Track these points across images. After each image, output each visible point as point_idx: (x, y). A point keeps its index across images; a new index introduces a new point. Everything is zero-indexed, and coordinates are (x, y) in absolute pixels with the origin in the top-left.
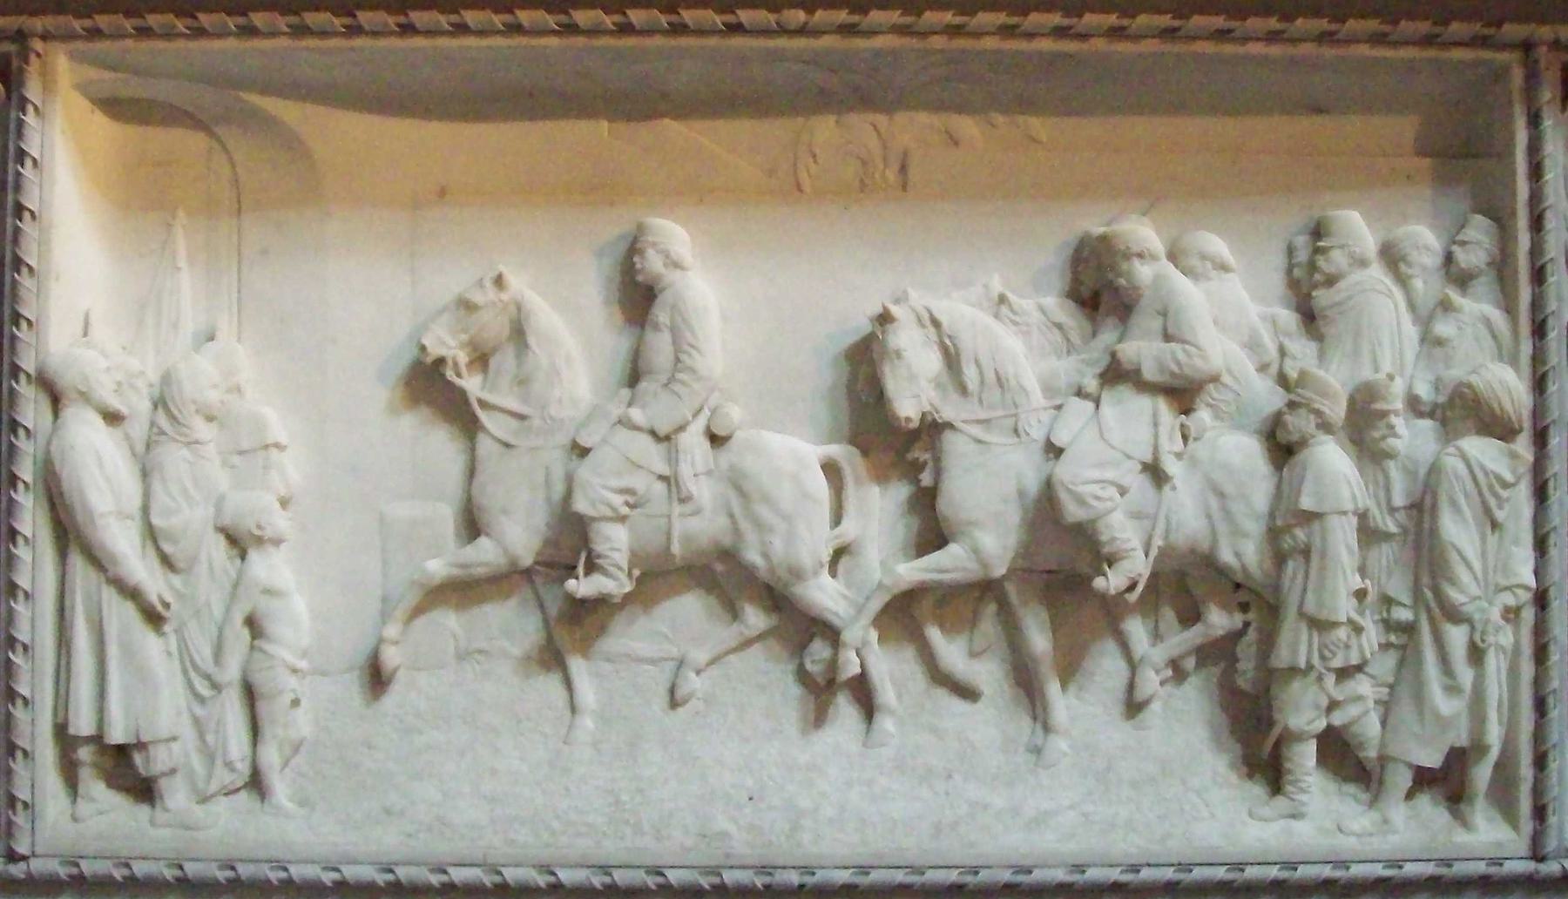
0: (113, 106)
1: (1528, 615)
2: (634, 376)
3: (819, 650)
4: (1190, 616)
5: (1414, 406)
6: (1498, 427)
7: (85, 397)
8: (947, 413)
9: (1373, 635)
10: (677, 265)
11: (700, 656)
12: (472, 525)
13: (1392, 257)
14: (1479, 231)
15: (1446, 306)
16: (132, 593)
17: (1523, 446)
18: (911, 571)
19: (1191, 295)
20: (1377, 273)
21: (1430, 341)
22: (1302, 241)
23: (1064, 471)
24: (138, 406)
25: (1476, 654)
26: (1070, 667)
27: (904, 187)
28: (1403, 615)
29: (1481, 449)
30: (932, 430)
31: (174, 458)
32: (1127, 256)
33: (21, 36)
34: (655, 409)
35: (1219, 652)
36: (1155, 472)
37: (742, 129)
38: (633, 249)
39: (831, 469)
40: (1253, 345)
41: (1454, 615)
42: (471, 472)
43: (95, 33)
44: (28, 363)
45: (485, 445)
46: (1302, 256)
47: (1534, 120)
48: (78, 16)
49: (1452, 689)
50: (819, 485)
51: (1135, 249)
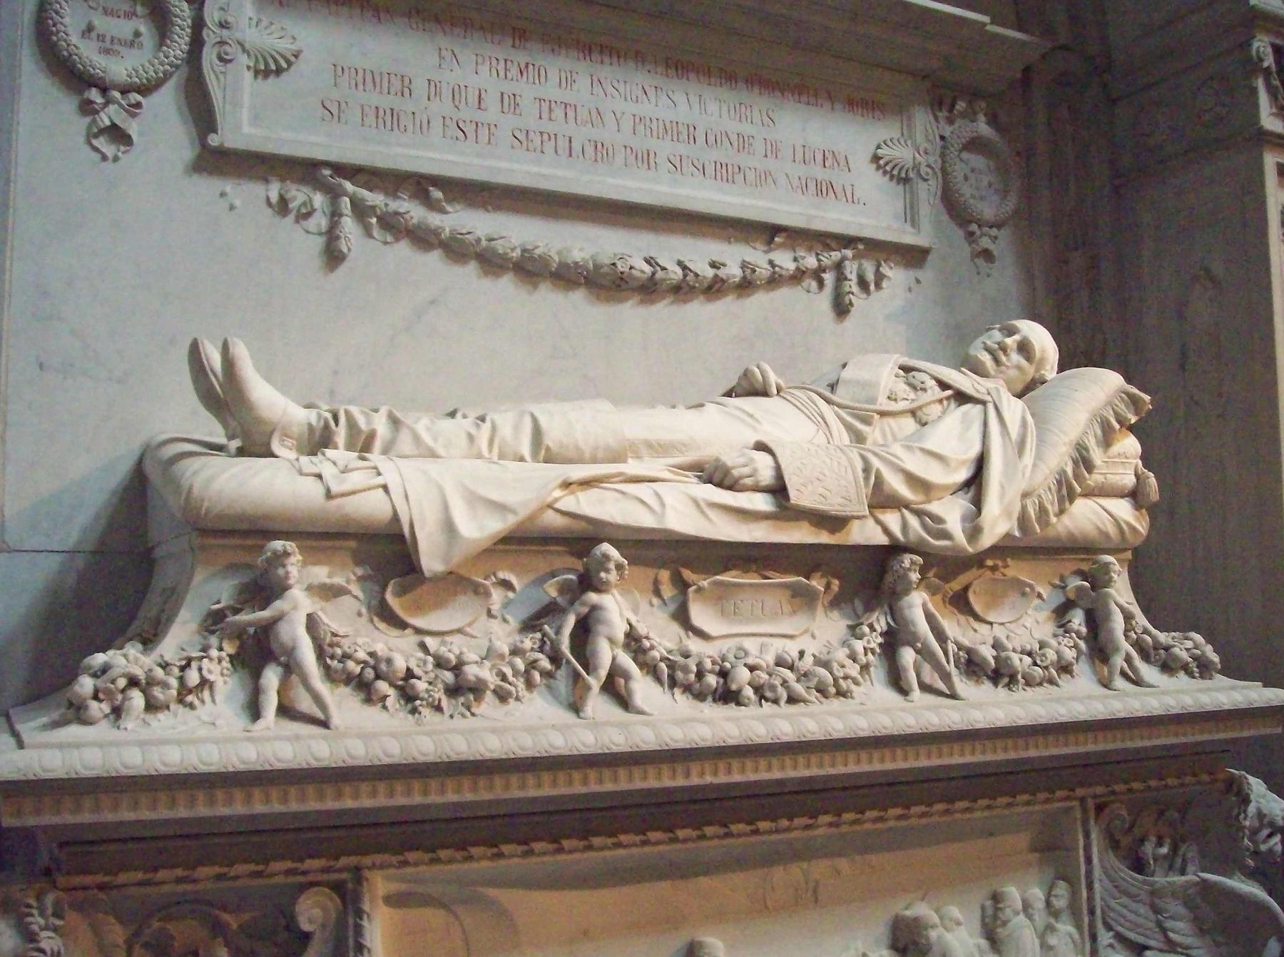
14: (1062, 889)
22: (989, 903)
27: (816, 901)
32: (926, 929)
33: (358, 869)
37: (738, 879)
43: (405, 863)
46: (990, 912)
48: (395, 854)
51: (931, 923)
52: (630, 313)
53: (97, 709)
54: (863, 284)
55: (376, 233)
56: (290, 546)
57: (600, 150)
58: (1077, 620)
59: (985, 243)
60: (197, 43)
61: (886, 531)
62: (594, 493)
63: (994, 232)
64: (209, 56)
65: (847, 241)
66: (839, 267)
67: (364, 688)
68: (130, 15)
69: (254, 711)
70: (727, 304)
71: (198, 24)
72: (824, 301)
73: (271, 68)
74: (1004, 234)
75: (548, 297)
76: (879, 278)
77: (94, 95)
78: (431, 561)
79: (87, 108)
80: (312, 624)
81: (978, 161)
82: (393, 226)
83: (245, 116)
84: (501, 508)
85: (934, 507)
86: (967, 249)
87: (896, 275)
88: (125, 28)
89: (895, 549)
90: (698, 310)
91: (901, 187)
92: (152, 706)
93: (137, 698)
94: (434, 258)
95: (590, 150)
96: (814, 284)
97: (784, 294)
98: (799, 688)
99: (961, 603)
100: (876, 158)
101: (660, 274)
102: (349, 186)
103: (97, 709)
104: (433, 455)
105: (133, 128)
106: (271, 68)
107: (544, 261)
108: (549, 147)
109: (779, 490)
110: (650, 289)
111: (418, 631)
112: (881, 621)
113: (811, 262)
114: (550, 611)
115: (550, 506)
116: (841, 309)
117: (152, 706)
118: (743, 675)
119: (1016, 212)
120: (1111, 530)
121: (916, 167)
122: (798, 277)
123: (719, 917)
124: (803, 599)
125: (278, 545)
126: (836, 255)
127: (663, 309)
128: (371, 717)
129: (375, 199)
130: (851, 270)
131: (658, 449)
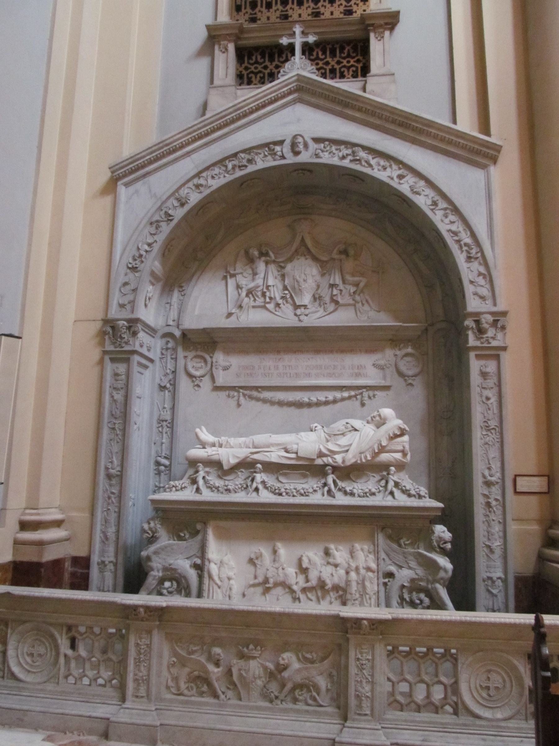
1: (377, 594)
2: (274, 561)
3: (294, 594)
4: (337, 592)
6: (373, 572)
7: (213, 562)
8: (309, 567)
9: (358, 596)
10: (279, 548)
11: (280, 594)
12: (255, 577)
13: (362, 550)
14: (372, 546)
15: (368, 556)
16: (217, 584)
17: (376, 574)
19: (337, 554)
21: (366, 560)
23: (322, 574)
24: (219, 562)
25: (370, 599)
26: (323, 598)
28: (361, 593)
29: (370, 574)
30: (307, 569)
31: (222, 569)
34: (277, 565)
35: (341, 597)
36: (332, 575)
39: (296, 573)
40: (345, 560)
41: (367, 594)
42: (256, 571)
44: (207, 558)
45: (258, 570)
47: (378, 534)
49: (367, 603)
50: (294, 574)
52: (305, 411)
53: (168, 490)
54: (369, 398)
55: (248, 399)
56: (201, 464)
57: (297, 375)
58: (383, 483)
59: (410, 381)
60: (212, 365)
61: (323, 461)
63: (414, 378)
64: (214, 369)
66: (362, 393)
68: (200, 362)
69: (192, 491)
71: (212, 363)
72: (358, 403)
73: (226, 369)
75: (285, 409)
76: (374, 396)
78: (226, 467)
79: (193, 381)
80: (204, 478)
82: (251, 397)
84: (238, 457)
86: (404, 384)
88: (199, 365)
89: (326, 465)
90: (323, 409)
91: (382, 371)
92: (177, 490)
93: (174, 489)
94: (259, 403)
95: (295, 376)
97: (346, 402)
98: (295, 494)
100: (374, 365)
101: (311, 402)
102: (241, 391)
103: (168, 490)
105: (201, 384)
106: (226, 369)
107: (283, 401)
108: (285, 376)
109: (297, 453)
110: (309, 405)
111: (225, 480)
113: (353, 393)
114: (250, 476)
115: (248, 457)
116: (363, 405)
118: (283, 490)
120: (393, 460)
121: (385, 365)
122: (350, 398)
123: (282, 539)
125: (199, 464)
126: (360, 391)
127: (313, 410)
128: (212, 494)
130: (366, 394)
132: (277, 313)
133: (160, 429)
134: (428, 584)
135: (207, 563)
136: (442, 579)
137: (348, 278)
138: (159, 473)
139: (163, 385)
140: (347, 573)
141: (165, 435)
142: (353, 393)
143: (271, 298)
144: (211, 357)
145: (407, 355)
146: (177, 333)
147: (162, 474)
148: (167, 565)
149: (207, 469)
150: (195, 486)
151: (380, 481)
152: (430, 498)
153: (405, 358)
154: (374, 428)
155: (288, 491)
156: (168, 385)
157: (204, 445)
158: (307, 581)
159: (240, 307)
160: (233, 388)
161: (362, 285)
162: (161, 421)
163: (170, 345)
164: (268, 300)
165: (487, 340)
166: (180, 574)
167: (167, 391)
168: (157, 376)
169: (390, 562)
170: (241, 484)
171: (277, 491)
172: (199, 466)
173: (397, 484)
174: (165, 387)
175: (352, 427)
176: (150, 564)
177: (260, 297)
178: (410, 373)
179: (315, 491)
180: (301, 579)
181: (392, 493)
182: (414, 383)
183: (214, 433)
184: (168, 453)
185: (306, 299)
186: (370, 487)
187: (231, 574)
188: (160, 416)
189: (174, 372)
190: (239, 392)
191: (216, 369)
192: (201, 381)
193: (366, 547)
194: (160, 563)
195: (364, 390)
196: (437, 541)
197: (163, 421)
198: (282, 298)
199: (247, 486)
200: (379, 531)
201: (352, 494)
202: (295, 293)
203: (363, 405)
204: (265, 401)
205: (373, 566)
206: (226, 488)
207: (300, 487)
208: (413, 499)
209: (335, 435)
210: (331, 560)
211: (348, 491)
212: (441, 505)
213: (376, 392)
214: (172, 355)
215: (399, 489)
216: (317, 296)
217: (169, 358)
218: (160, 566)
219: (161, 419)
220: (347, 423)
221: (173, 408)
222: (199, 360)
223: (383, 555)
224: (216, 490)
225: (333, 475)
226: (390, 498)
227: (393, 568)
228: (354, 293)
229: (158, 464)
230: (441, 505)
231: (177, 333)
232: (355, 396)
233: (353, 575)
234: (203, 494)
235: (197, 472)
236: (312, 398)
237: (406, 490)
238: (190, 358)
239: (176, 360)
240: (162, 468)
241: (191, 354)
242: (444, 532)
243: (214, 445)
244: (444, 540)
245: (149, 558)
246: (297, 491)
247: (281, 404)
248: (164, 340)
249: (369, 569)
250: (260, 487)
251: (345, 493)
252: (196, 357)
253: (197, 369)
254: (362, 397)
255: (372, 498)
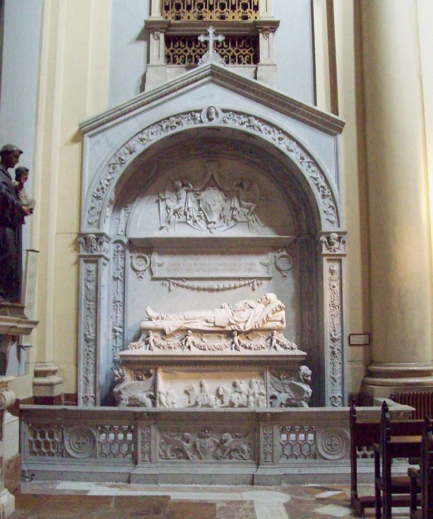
0: (163, 372)
2: (201, 391)
5: (258, 393)
6: (263, 395)
8: (224, 394)
12: (189, 402)
13: (257, 383)
14: (263, 381)
18: (221, 405)
19: (241, 386)
20: (256, 384)
21: (259, 389)
24: (165, 394)
30: (223, 395)
31: (168, 398)
34: (202, 394)
36: (238, 398)
38: (201, 382)
42: (189, 398)
45: (190, 397)
50: (215, 399)
52: (215, 294)
54: (258, 285)
57: (210, 270)
58: (269, 341)
59: (285, 274)
62: (189, 324)
65: (254, 278)
66: (253, 282)
67: (159, 347)
69: (146, 349)
70: (232, 290)
71: (150, 261)
72: (250, 288)
73: (160, 265)
74: (289, 272)
75: (202, 293)
76: (261, 284)
77: (138, 273)
78: (167, 333)
79: (137, 274)
80: (153, 340)
81: (284, 259)
82: (178, 285)
83: (157, 272)
84: (176, 326)
85: (239, 325)
86: (281, 276)
87: (264, 282)
88: (141, 263)
89: (233, 331)
90: (227, 293)
91: (266, 267)
93: (134, 348)
94: (184, 289)
96: (248, 286)
97: (243, 288)
98: (214, 349)
99: (248, 338)
102: (171, 280)
103: (130, 348)
104: (171, 320)
106: (160, 265)
109: (214, 323)
110: (218, 290)
112: (231, 340)
114: (183, 339)
116: (253, 290)
117: (136, 348)
118: (206, 347)
119: (292, 268)
120: (276, 327)
121: (268, 263)
122: (245, 285)
123: (206, 378)
124: (220, 337)
125: (150, 331)
126: (252, 281)
127: (220, 293)
129: (175, 282)
130: (255, 283)
131: (201, 318)
132: (195, 227)
133: (115, 307)
134: (297, 401)
135: (158, 394)
136: (306, 398)
137: (244, 203)
138: (116, 337)
139: (116, 277)
140: (248, 397)
141: (119, 311)
142: (247, 282)
143: (190, 216)
144: (150, 257)
145: (283, 256)
146: (125, 241)
147: (118, 338)
148: (131, 396)
149: (155, 334)
150: (148, 346)
151: (267, 340)
152: (298, 349)
153: (281, 259)
154: (264, 306)
155: (210, 347)
156: (120, 277)
157: (150, 319)
158: (222, 402)
159: (169, 222)
160: (166, 279)
161: (253, 208)
162: (115, 302)
163: (120, 249)
164: (188, 218)
165: (334, 250)
166: (140, 402)
167: (119, 281)
168: (112, 270)
169: (274, 390)
170: (178, 343)
171: (202, 348)
172: (149, 333)
173: (278, 342)
174: (117, 278)
175: (249, 306)
176: (121, 396)
177: (183, 215)
178: (285, 268)
179: (226, 347)
180: (219, 401)
181: (275, 347)
182: (287, 276)
183: (155, 309)
184: (122, 324)
185: (215, 218)
186: (261, 344)
187: (174, 401)
188: (115, 298)
189: (124, 268)
190: (170, 281)
191: (154, 265)
192: (143, 274)
193: (259, 381)
194: (127, 395)
195: (255, 280)
196: (302, 376)
197: (117, 302)
198: (198, 216)
199: (182, 345)
200: (267, 370)
201: (250, 348)
202: (208, 214)
203: (253, 290)
204: (187, 288)
205: (264, 392)
206: (168, 346)
207: (217, 345)
208: (288, 350)
209: (238, 311)
210: (238, 390)
211: (248, 346)
212: (305, 353)
213: (262, 281)
214: (122, 255)
215: (279, 344)
216: (222, 215)
217: (120, 257)
218: (127, 398)
219: (116, 300)
220: (246, 303)
221: (124, 293)
222: (141, 259)
223: (269, 385)
224: (162, 348)
225: (238, 337)
226: (273, 350)
227: (276, 393)
228: (248, 213)
229: (115, 331)
230: (305, 353)
231: (125, 241)
232: (249, 284)
233: (251, 398)
234: (154, 350)
235: (148, 336)
236: (219, 286)
237: (284, 345)
238: (134, 258)
239: (125, 259)
240: (118, 334)
241: (135, 255)
242: (307, 370)
243: (158, 318)
244: (307, 375)
245: (120, 393)
246: (216, 347)
247: (198, 289)
248: (116, 245)
249: (261, 394)
250: (191, 345)
251: (246, 347)
252: (139, 257)
253: (140, 266)
254: (253, 284)
255: (262, 350)
